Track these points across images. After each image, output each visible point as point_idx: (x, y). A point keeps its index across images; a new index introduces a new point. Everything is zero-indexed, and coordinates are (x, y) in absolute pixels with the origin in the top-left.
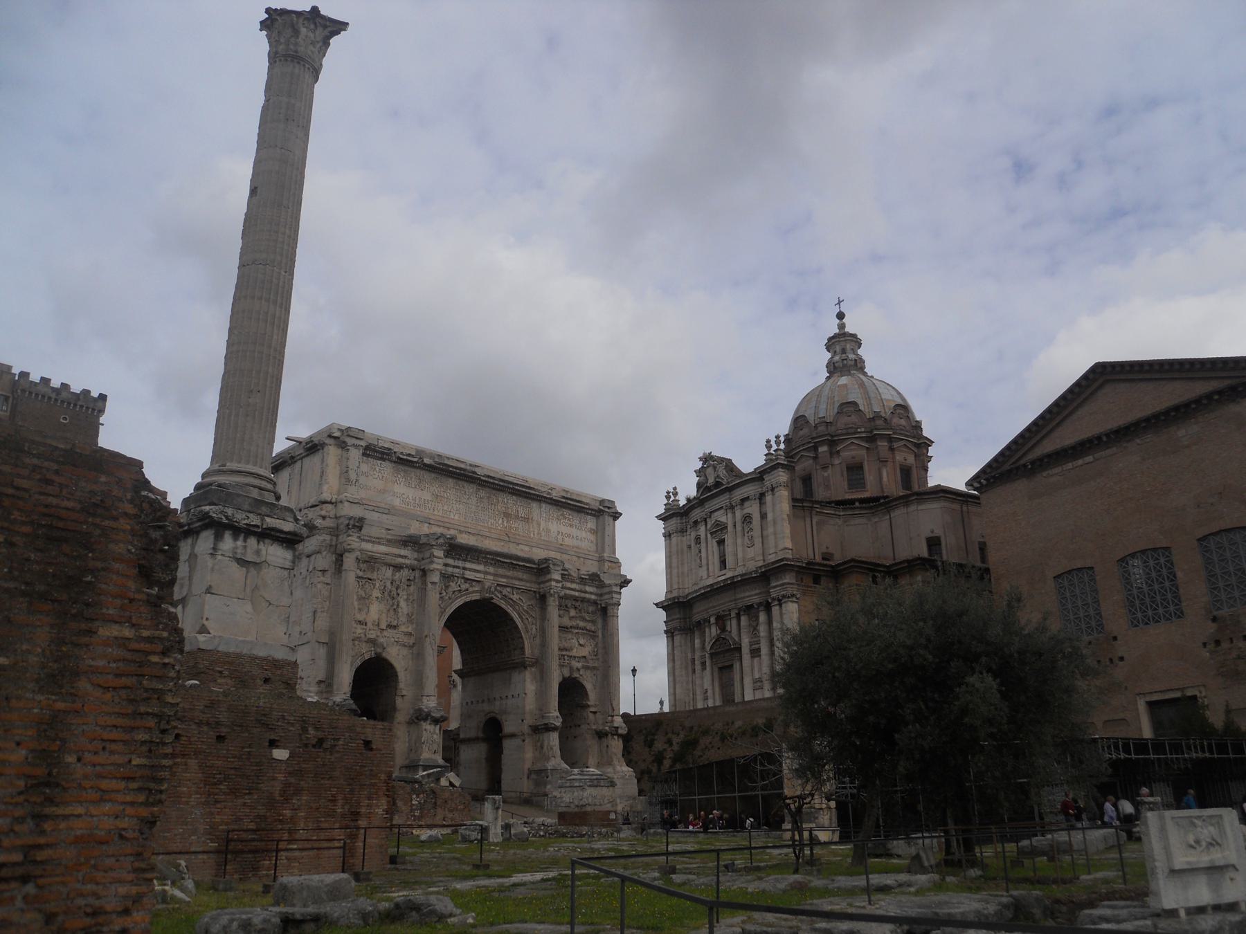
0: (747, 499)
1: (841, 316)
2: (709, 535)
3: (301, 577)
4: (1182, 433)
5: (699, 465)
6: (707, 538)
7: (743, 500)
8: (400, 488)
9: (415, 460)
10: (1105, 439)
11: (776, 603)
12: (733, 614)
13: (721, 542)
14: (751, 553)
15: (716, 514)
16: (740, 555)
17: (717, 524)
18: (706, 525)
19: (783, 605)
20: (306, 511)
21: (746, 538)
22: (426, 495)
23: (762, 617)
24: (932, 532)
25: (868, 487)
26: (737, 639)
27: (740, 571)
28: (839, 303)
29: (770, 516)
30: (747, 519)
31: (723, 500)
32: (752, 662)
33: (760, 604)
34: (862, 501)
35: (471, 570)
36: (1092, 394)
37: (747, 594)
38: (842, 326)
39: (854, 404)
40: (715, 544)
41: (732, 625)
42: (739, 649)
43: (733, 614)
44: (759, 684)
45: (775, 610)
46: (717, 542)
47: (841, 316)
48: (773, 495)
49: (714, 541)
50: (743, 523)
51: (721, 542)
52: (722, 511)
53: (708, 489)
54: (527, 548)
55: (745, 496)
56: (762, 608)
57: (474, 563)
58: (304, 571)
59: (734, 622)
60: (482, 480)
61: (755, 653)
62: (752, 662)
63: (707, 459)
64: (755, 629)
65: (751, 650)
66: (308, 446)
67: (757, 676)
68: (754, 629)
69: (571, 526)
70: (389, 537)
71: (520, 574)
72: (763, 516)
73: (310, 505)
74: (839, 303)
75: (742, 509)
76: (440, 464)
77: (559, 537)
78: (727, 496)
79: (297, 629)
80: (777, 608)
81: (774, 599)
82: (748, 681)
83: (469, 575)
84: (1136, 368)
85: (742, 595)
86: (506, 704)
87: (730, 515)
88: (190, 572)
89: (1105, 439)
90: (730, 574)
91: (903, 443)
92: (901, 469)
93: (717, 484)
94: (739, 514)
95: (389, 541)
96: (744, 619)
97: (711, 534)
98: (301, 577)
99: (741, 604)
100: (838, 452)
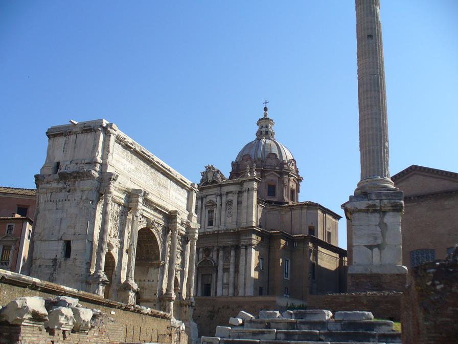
0: (231, 192)
1: (266, 109)
2: (204, 207)
3: (76, 201)
4: (446, 203)
5: (204, 170)
6: (202, 208)
7: (228, 193)
8: (124, 161)
9: (133, 147)
10: (412, 198)
11: (244, 247)
12: (215, 249)
13: (211, 212)
14: (229, 220)
15: (209, 197)
16: (223, 220)
17: (211, 202)
18: (202, 202)
19: (248, 249)
20: (82, 165)
21: (227, 212)
22: (133, 167)
23: (233, 253)
24: (312, 224)
25: (277, 196)
26: (216, 261)
27: (222, 227)
28: (266, 103)
29: (244, 204)
30: (229, 203)
31: (216, 190)
32: (223, 274)
33: (232, 246)
34: (276, 203)
35: (146, 211)
36: (407, 178)
37: (225, 240)
38: (265, 115)
39: (275, 154)
40: (207, 213)
41: (214, 255)
42: (217, 267)
43: (215, 249)
44: (226, 286)
45: (243, 251)
46: (209, 211)
47: (266, 109)
48: (248, 193)
49: (207, 211)
50: (226, 204)
51: (211, 212)
52: (214, 196)
53: (207, 183)
54: (166, 204)
55: (230, 191)
56: (233, 248)
57: (146, 207)
58: (78, 199)
59: (215, 253)
60: (155, 165)
61: (226, 270)
62: (223, 274)
63: (209, 169)
64: (227, 258)
65: (223, 269)
66: (86, 128)
67: (225, 281)
68: (226, 258)
69: (180, 194)
70: (120, 188)
71: (161, 217)
72: (240, 203)
73: (86, 161)
74: (266, 103)
75: (227, 197)
76: (142, 151)
77: (176, 200)
78: (219, 188)
79: (72, 231)
80: (244, 250)
81: (243, 245)
82: (220, 284)
83: (145, 214)
84: (449, 175)
85: (222, 240)
86: (144, 284)
87: (219, 199)
88: (381, 232)
89: (412, 198)
90: (216, 229)
91: (293, 178)
92: (291, 190)
93: (213, 182)
94: (224, 198)
95: (119, 189)
96: (221, 253)
97: (205, 206)
98: (76, 201)
99: (221, 245)
100: (265, 176)
